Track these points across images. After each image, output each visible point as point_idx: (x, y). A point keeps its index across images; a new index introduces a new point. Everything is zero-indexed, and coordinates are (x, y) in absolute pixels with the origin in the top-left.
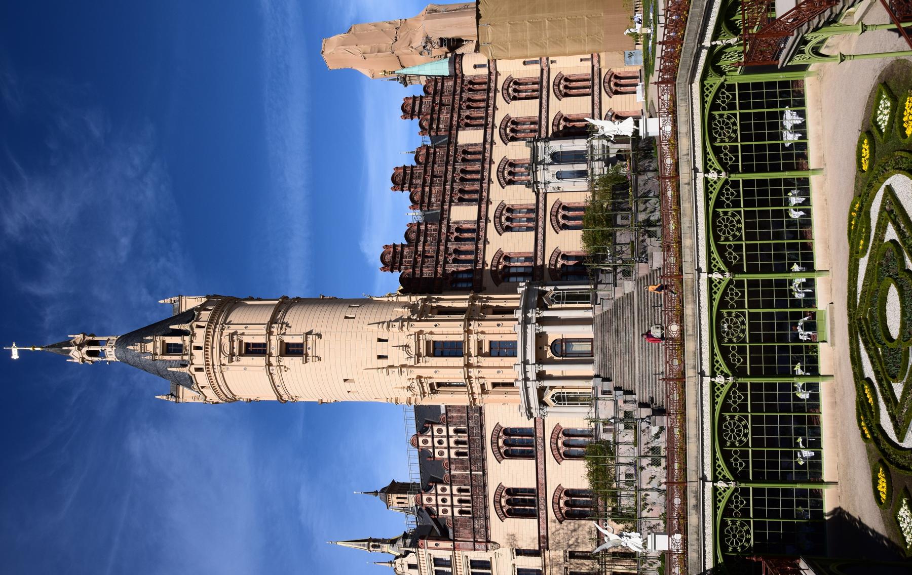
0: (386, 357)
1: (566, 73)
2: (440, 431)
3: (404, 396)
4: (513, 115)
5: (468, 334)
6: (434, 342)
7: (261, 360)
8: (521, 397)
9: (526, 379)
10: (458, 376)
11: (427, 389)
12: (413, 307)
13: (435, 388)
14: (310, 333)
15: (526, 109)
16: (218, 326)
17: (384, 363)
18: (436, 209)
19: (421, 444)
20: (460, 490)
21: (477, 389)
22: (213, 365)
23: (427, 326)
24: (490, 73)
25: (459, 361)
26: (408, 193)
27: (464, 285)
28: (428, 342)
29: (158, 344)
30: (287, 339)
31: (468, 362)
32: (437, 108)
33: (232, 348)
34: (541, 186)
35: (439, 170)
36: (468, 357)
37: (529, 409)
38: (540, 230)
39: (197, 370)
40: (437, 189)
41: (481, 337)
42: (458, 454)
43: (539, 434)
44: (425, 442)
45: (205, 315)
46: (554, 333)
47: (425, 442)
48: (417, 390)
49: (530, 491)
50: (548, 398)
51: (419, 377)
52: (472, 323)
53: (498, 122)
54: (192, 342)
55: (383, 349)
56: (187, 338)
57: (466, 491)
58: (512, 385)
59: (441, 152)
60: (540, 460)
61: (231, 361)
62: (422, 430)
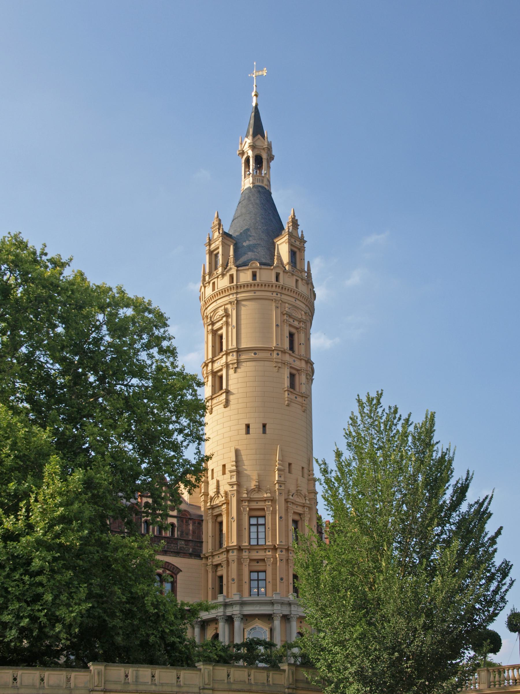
5: (272, 549)
6: (264, 517)
9: (226, 605)
16: (279, 295)
22: (237, 293)
28: (264, 509)
31: (242, 550)
36: (249, 549)
52: (284, 553)
58: (221, 592)
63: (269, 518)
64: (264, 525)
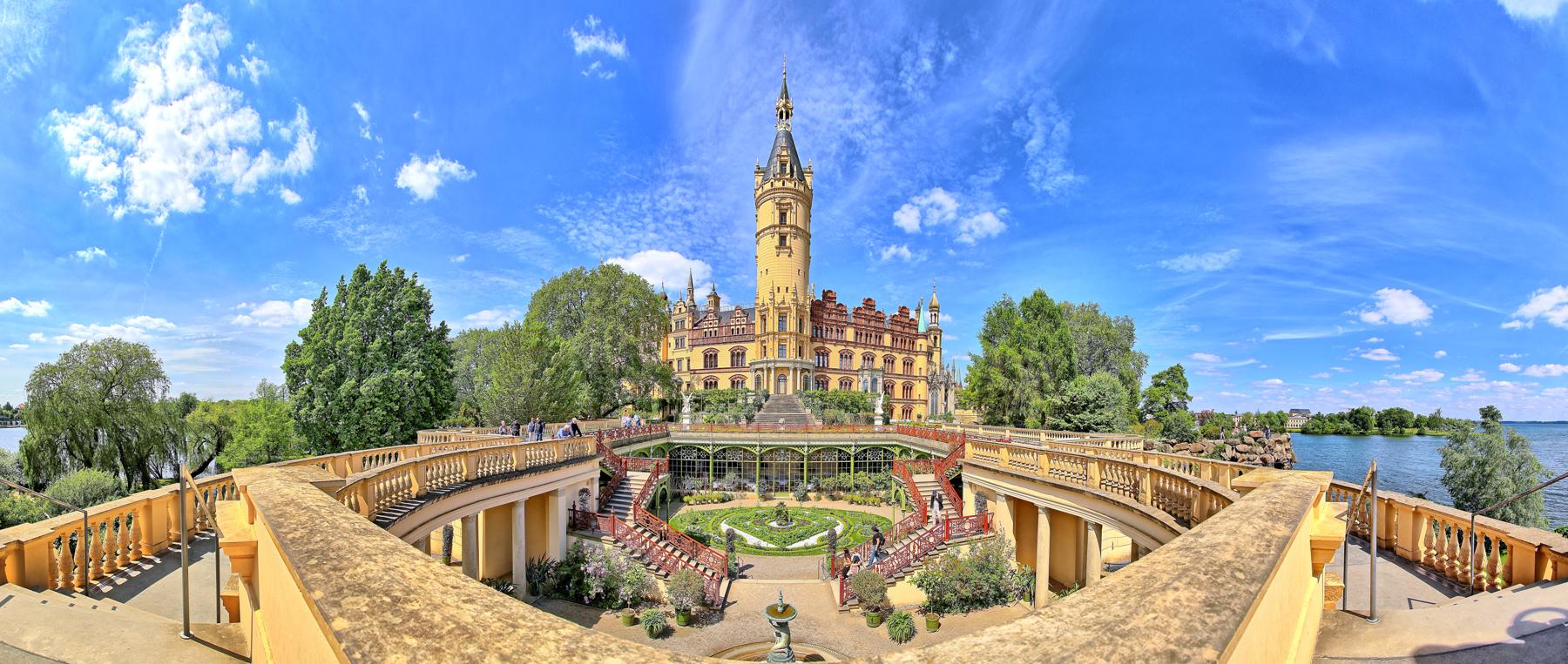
2: (744, 321)
3: (760, 302)
9: (767, 362)
10: (769, 328)
12: (803, 306)
13: (764, 318)
14: (791, 252)
17: (776, 291)
18: (853, 320)
20: (716, 332)
21: (763, 338)
23: (794, 313)
25: (776, 330)
26: (862, 306)
30: (788, 238)
33: (784, 204)
34: (861, 373)
35: (872, 323)
37: (755, 363)
40: (863, 321)
41: (788, 340)
43: (743, 369)
44: (738, 313)
45: (802, 188)
46: (790, 378)
49: (717, 366)
51: (768, 309)
54: (787, 179)
55: (783, 290)
59: (881, 325)
60: (730, 370)
61: (777, 204)
62: (743, 311)
63: (788, 318)
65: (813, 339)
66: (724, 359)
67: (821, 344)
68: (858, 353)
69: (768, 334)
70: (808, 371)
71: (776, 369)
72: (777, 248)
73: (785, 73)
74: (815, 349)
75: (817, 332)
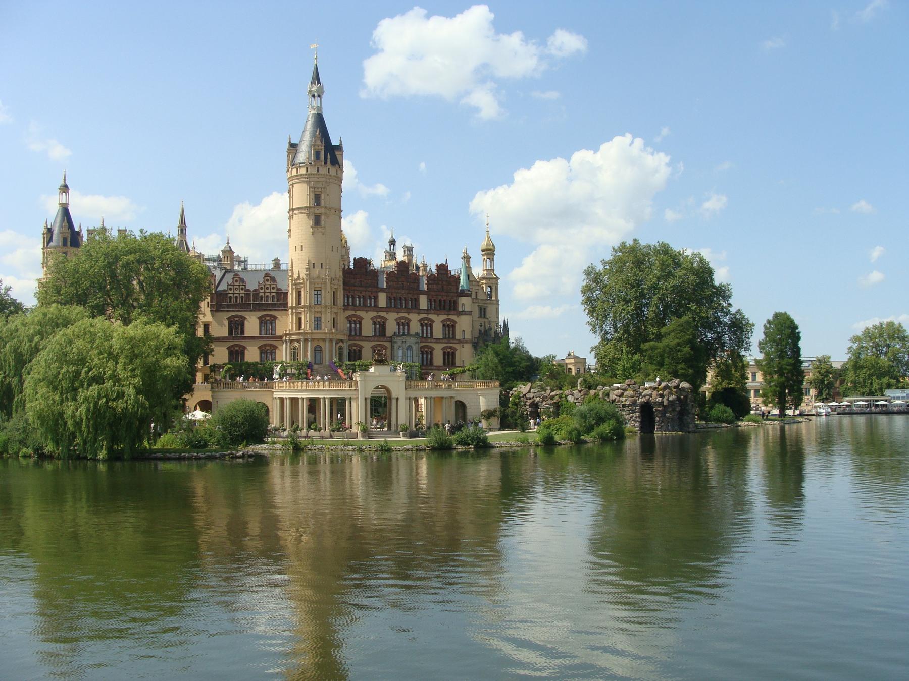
0: (314, 268)
1: (457, 353)
4: (435, 325)
7: (313, 204)
8: (295, 331)
9: (305, 334)
10: (305, 301)
11: (299, 286)
15: (438, 331)
19: (266, 278)
24: (460, 312)
27: (346, 301)
29: (320, 147)
30: (323, 218)
32: (440, 283)
38: (373, 338)
39: (307, 168)
41: (323, 313)
42: (261, 296)
47: (267, 280)
48: (299, 282)
49: (242, 332)
50: (296, 344)
53: (431, 316)
55: (318, 266)
56: (323, 163)
57: (242, 301)
64: (321, 294)
65: (346, 307)
66: (252, 326)
67: (352, 313)
68: (391, 318)
69: (304, 307)
70: (342, 341)
71: (313, 340)
72: (311, 227)
73: (316, 59)
74: (347, 318)
75: (348, 300)
